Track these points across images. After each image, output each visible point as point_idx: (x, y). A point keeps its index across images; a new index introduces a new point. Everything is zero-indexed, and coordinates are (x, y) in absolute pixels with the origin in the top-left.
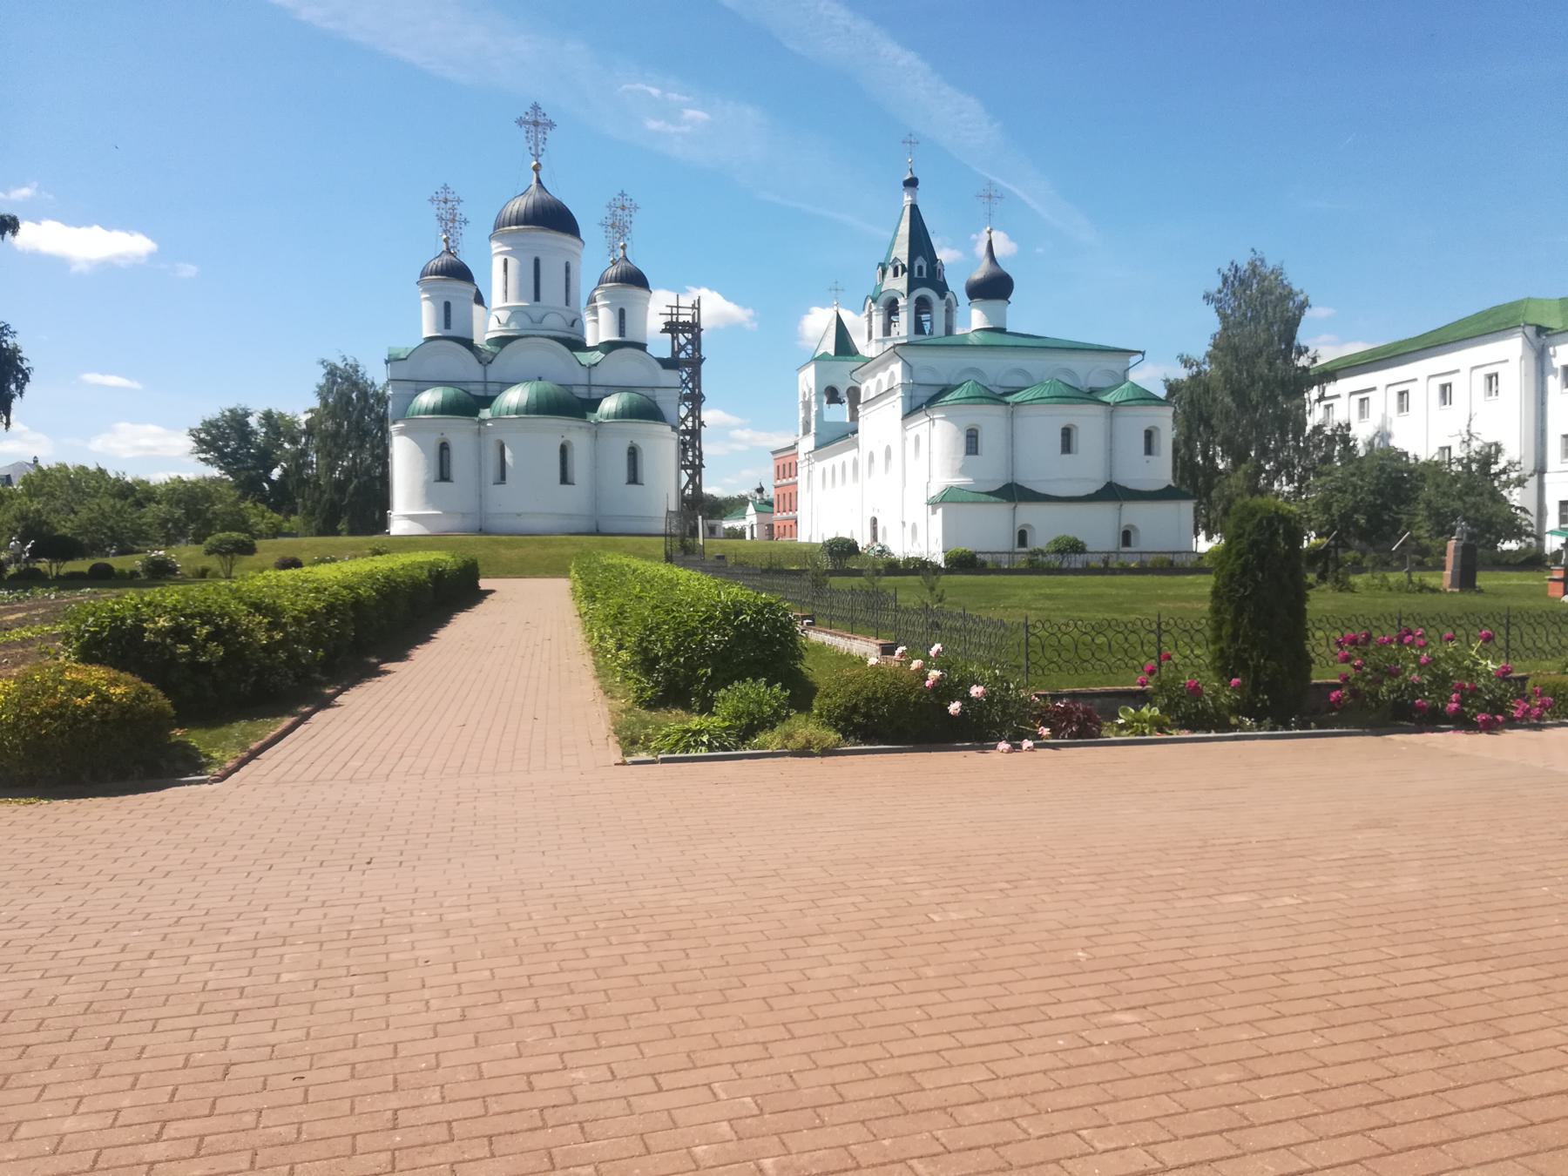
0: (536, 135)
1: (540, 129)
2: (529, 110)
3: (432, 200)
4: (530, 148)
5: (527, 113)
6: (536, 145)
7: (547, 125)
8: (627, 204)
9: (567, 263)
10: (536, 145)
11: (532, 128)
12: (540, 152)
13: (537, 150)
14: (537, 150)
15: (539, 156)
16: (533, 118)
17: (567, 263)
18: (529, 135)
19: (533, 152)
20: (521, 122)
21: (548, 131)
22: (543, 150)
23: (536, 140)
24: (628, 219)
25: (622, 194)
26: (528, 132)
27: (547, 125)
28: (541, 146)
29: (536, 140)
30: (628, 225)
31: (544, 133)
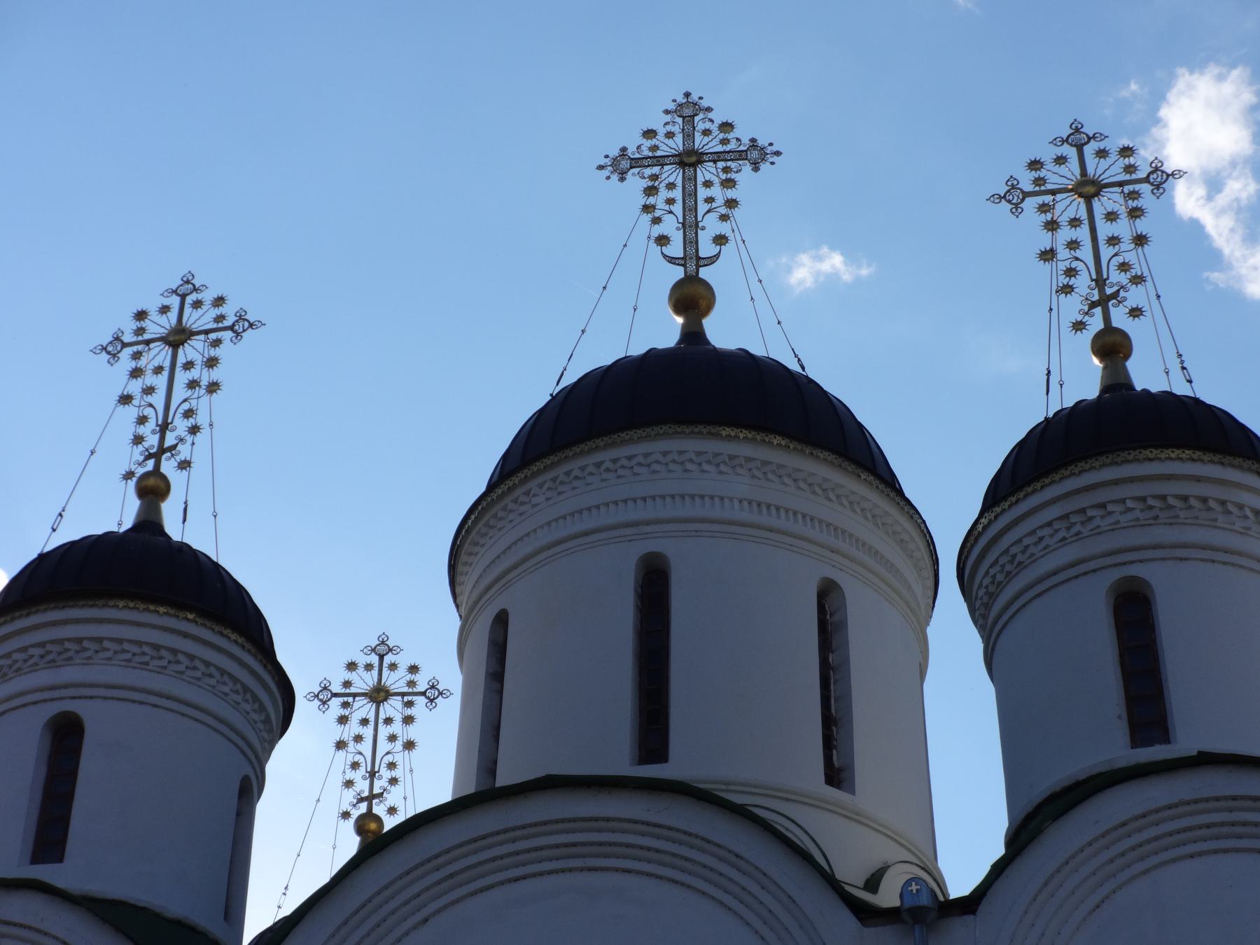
0: (690, 194)
1: (706, 172)
2: (658, 122)
3: (113, 348)
4: (662, 240)
5: (649, 134)
6: (691, 227)
7: (740, 155)
8: (1111, 170)
9: (828, 594)
10: (691, 227)
11: (673, 174)
12: (707, 248)
13: (691, 242)
14: (691, 242)
15: (700, 262)
16: (678, 143)
17: (828, 594)
18: (659, 200)
19: (676, 249)
20: (622, 164)
21: (744, 175)
22: (720, 240)
23: (690, 209)
24: (1123, 228)
25: (1078, 138)
26: (651, 191)
27: (740, 155)
28: (711, 226)
29: (690, 209)
30: (1129, 253)
31: (729, 183)
